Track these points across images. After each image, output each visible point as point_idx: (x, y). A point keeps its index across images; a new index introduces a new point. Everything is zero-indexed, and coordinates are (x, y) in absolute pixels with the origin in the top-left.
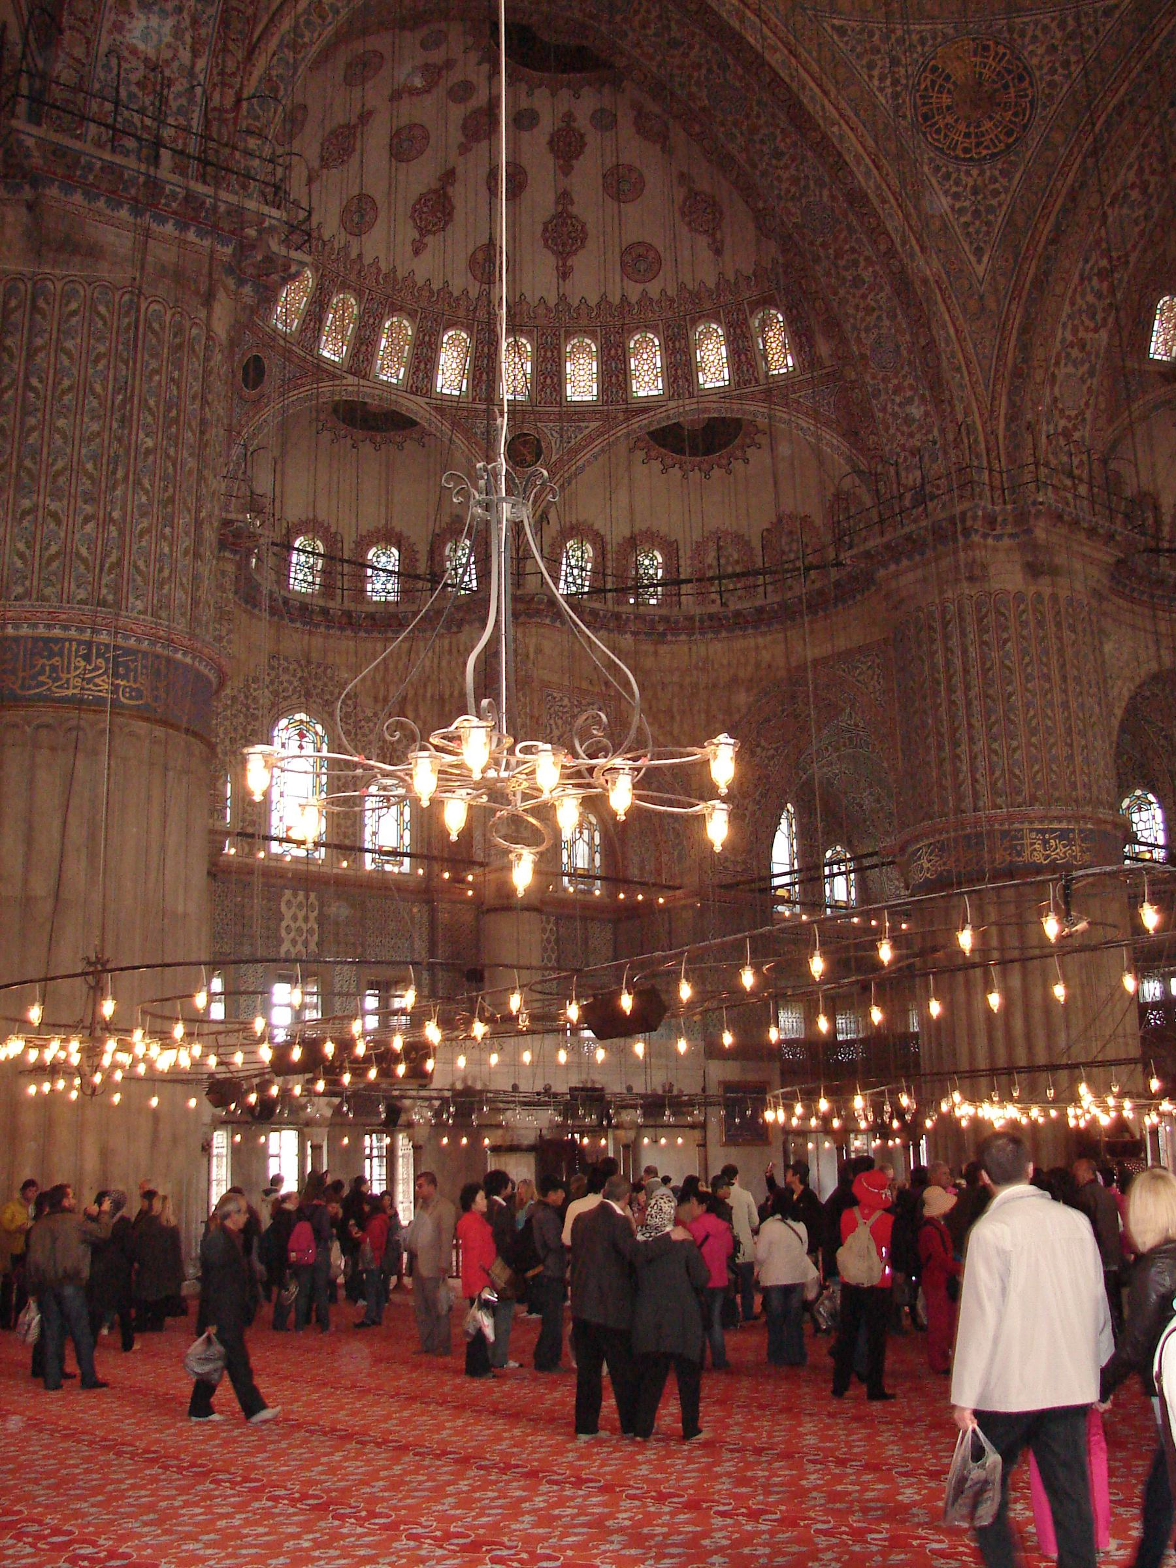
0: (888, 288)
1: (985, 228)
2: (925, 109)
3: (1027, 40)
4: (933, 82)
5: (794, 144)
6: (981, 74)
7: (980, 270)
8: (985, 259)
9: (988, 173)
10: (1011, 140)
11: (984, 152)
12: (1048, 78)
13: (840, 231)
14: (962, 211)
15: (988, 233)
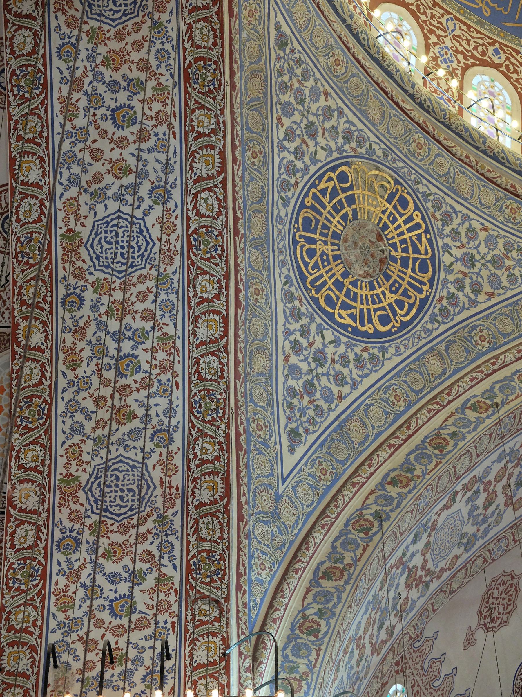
0: (178, 394)
1: (311, 412)
2: (311, 214)
3: (447, 230)
4: (334, 193)
5: (161, 119)
6: (385, 227)
7: (290, 461)
8: (300, 451)
9: (342, 349)
10: (382, 329)
11: (348, 321)
12: (452, 289)
13: (143, 278)
14: (294, 371)
15: (312, 422)
